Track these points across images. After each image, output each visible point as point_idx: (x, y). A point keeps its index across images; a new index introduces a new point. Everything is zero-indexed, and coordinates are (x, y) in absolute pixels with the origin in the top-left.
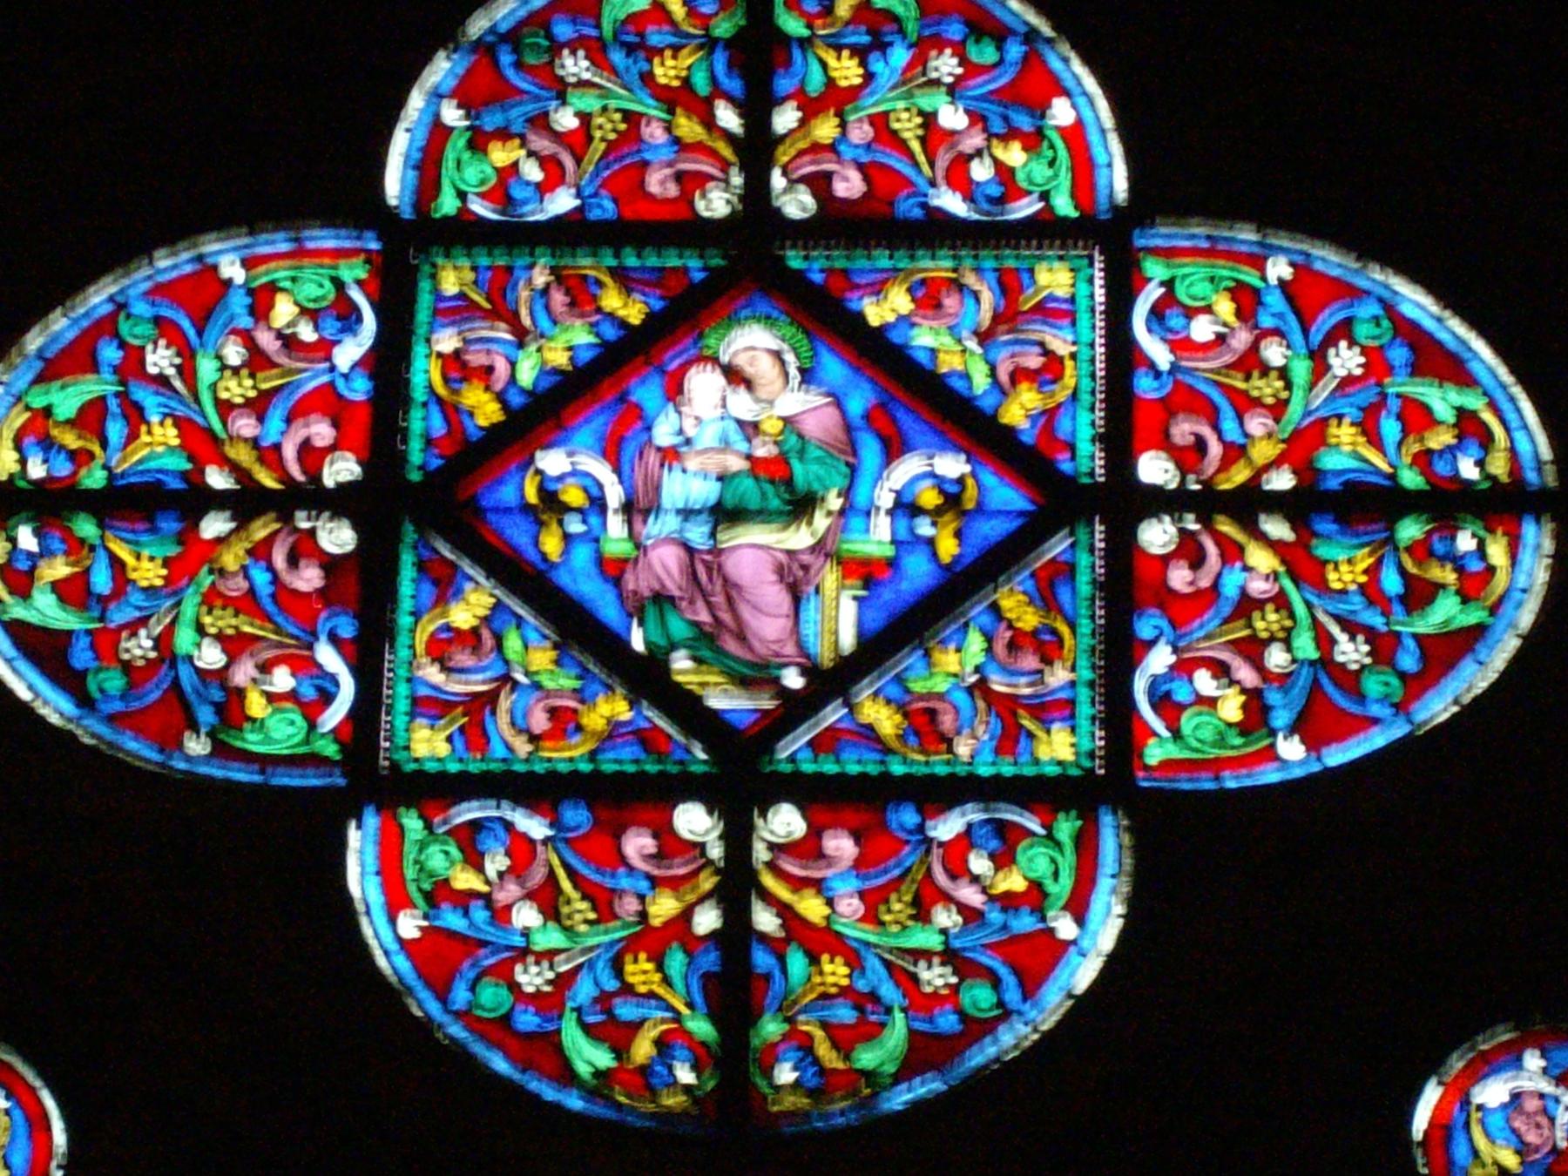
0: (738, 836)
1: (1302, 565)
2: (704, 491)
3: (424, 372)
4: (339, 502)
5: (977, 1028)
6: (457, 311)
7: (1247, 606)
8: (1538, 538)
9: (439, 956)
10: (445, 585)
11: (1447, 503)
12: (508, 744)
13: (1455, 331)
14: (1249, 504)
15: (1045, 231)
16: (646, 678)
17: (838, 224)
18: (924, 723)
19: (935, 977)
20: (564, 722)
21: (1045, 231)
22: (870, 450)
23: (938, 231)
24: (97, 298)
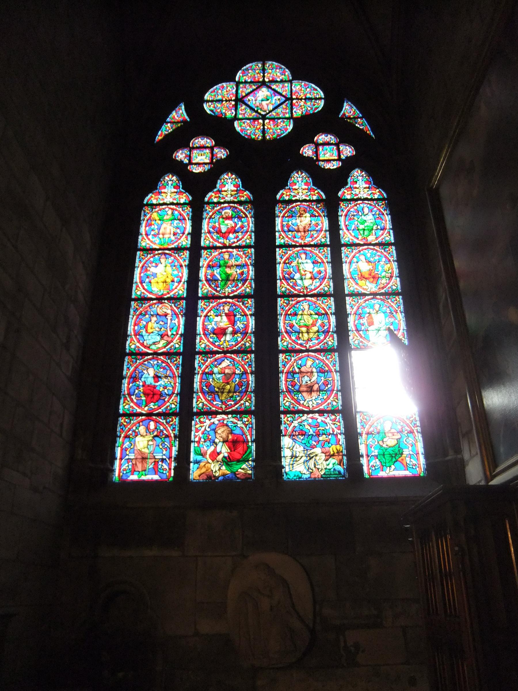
0: (264, 122)
1: (305, 103)
2: (261, 99)
3: (239, 92)
4: (234, 101)
5: (282, 134)
6: (242, 88)
7: (301, 106)
8: (323, 101)
9: (242, 130)
10: (242, 106)
11: (316, 99)
12: (246, 116)
13: (316, 87)
14: (301, 99)
15: (286, 81)
16: (257, 112)
17: (270, 81)
18: (277, 114)
19: (279, 131)
20: (251, 115)
21: (286, 81)
22: (273, 96)
23: (277, 82)
24: (215, 87)
